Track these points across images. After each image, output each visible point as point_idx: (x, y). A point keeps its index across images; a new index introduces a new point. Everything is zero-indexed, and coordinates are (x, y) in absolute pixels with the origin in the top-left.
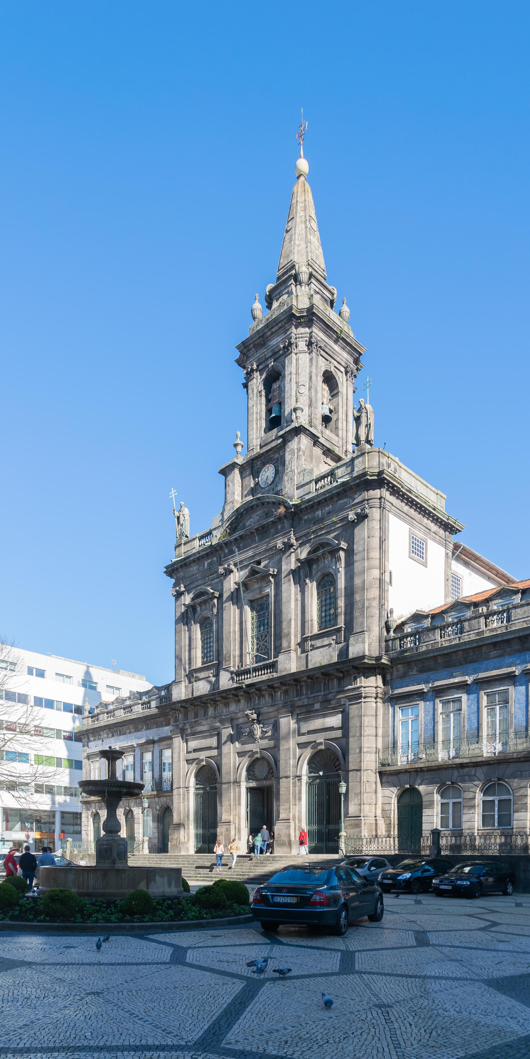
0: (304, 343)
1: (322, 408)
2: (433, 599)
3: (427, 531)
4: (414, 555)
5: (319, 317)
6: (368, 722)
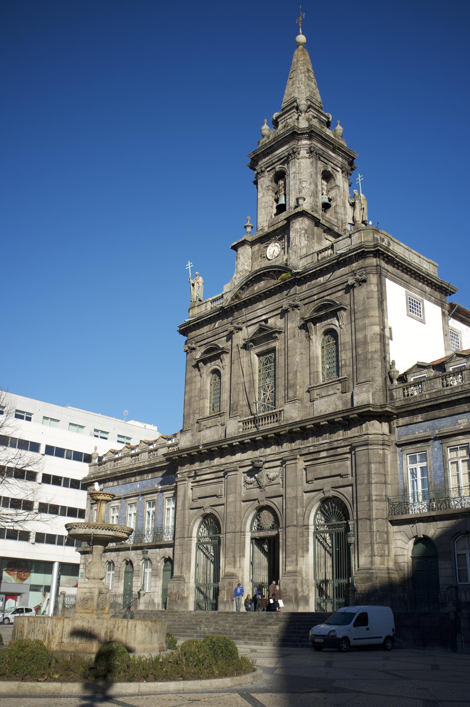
0: (306, 151)
1: (322, 198)
2: (435, 352)
3: (423, 293)
4: (412, 313)
5: (318, 134)
6: (376, 469)
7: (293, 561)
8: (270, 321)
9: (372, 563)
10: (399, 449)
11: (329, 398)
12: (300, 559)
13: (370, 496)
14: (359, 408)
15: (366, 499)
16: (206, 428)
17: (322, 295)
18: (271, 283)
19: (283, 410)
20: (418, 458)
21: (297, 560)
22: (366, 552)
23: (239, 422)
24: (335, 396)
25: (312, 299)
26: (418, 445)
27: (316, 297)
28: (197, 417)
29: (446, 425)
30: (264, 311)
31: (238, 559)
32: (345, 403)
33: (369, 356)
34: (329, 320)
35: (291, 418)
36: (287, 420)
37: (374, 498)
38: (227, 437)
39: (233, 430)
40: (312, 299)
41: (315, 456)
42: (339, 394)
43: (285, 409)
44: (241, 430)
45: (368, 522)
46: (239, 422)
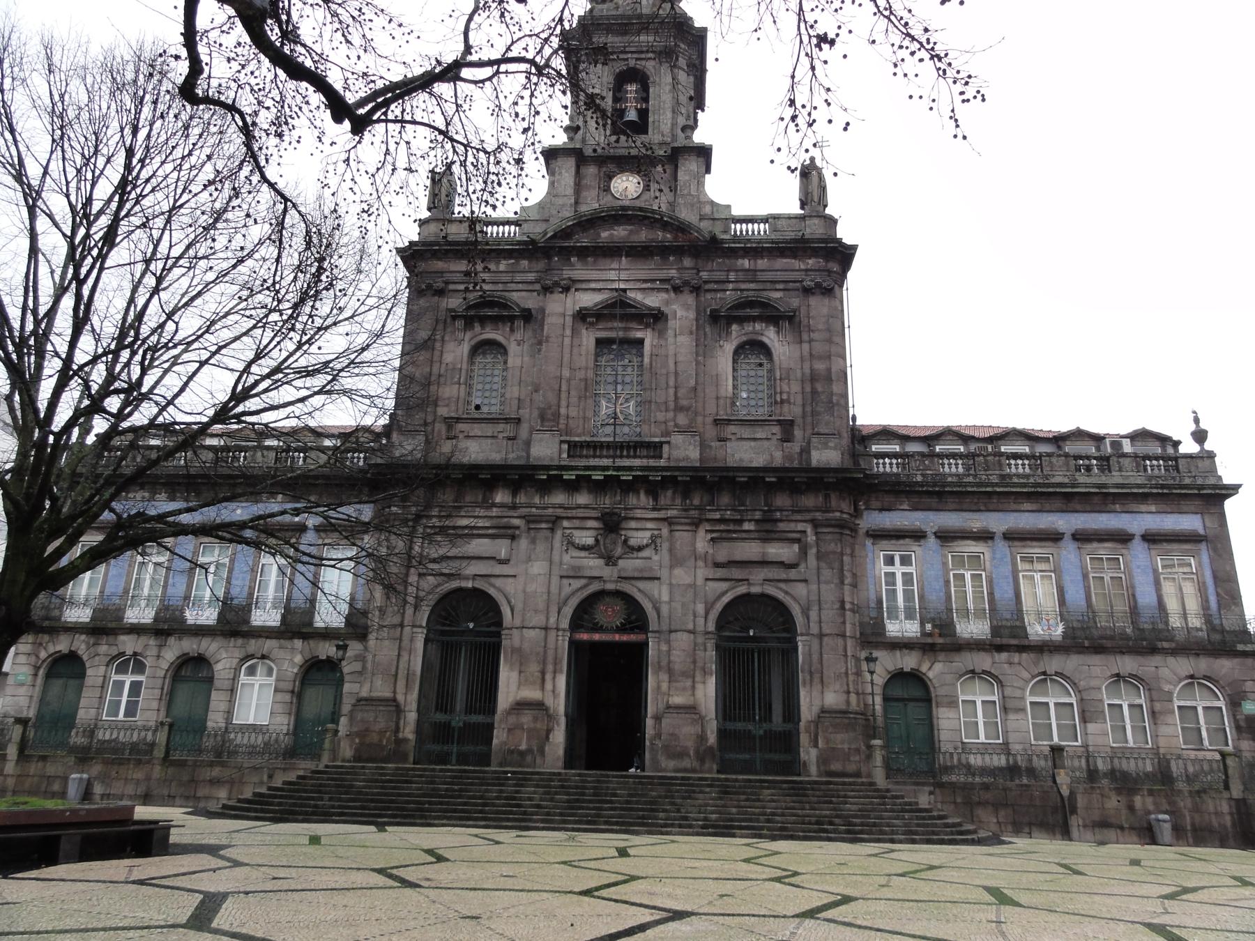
7: (684, 689)
8: (630, 294)
9: (848, 702)
10: (869, 542)
11: (759, 443)
12: (699, 686)
13: (843, 602)
14: (818, 470)
15: (837, 606)
16: (468, 437)
17: (743, 286)
18: (644, 236)
19: (668, 442)
20: (897, 560)
21: (693, 688)
22: (837, 687)
23: (562, 442)
24: (766, 443)
25: (724, 287)
26: (901, 542)
27: (731, 286)
28: (443, 411)
29: (951, 520)
30: (624, 275)
31: (548, 677)
32: (788, 457)
33: (835, 399)
34: (758, 326)
35: (687, 459)
36: (678, 460)
37: (848, 606)
38: (532, 461)
39: (549, 452)
40: (724, 287)
41: (731, 527)
42: (774, 442)
43: (673, 441)
44: (565, 455)
45: (840, 641)
46: (562, 442)
